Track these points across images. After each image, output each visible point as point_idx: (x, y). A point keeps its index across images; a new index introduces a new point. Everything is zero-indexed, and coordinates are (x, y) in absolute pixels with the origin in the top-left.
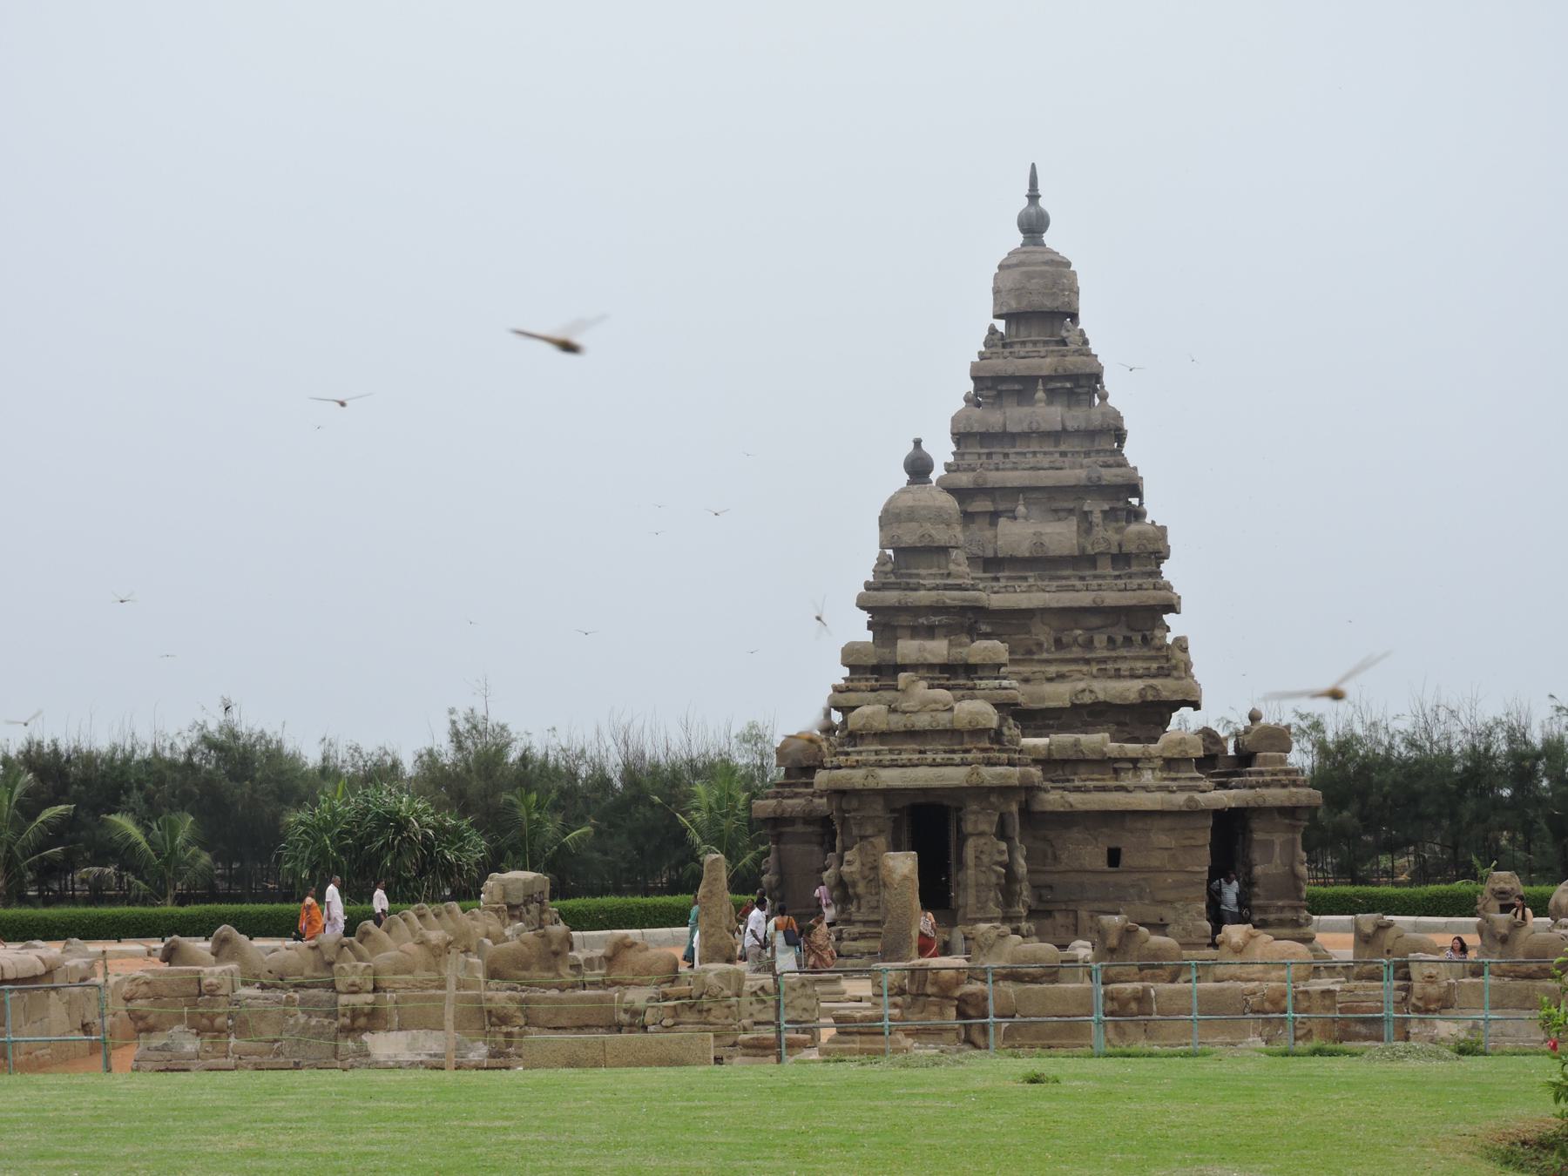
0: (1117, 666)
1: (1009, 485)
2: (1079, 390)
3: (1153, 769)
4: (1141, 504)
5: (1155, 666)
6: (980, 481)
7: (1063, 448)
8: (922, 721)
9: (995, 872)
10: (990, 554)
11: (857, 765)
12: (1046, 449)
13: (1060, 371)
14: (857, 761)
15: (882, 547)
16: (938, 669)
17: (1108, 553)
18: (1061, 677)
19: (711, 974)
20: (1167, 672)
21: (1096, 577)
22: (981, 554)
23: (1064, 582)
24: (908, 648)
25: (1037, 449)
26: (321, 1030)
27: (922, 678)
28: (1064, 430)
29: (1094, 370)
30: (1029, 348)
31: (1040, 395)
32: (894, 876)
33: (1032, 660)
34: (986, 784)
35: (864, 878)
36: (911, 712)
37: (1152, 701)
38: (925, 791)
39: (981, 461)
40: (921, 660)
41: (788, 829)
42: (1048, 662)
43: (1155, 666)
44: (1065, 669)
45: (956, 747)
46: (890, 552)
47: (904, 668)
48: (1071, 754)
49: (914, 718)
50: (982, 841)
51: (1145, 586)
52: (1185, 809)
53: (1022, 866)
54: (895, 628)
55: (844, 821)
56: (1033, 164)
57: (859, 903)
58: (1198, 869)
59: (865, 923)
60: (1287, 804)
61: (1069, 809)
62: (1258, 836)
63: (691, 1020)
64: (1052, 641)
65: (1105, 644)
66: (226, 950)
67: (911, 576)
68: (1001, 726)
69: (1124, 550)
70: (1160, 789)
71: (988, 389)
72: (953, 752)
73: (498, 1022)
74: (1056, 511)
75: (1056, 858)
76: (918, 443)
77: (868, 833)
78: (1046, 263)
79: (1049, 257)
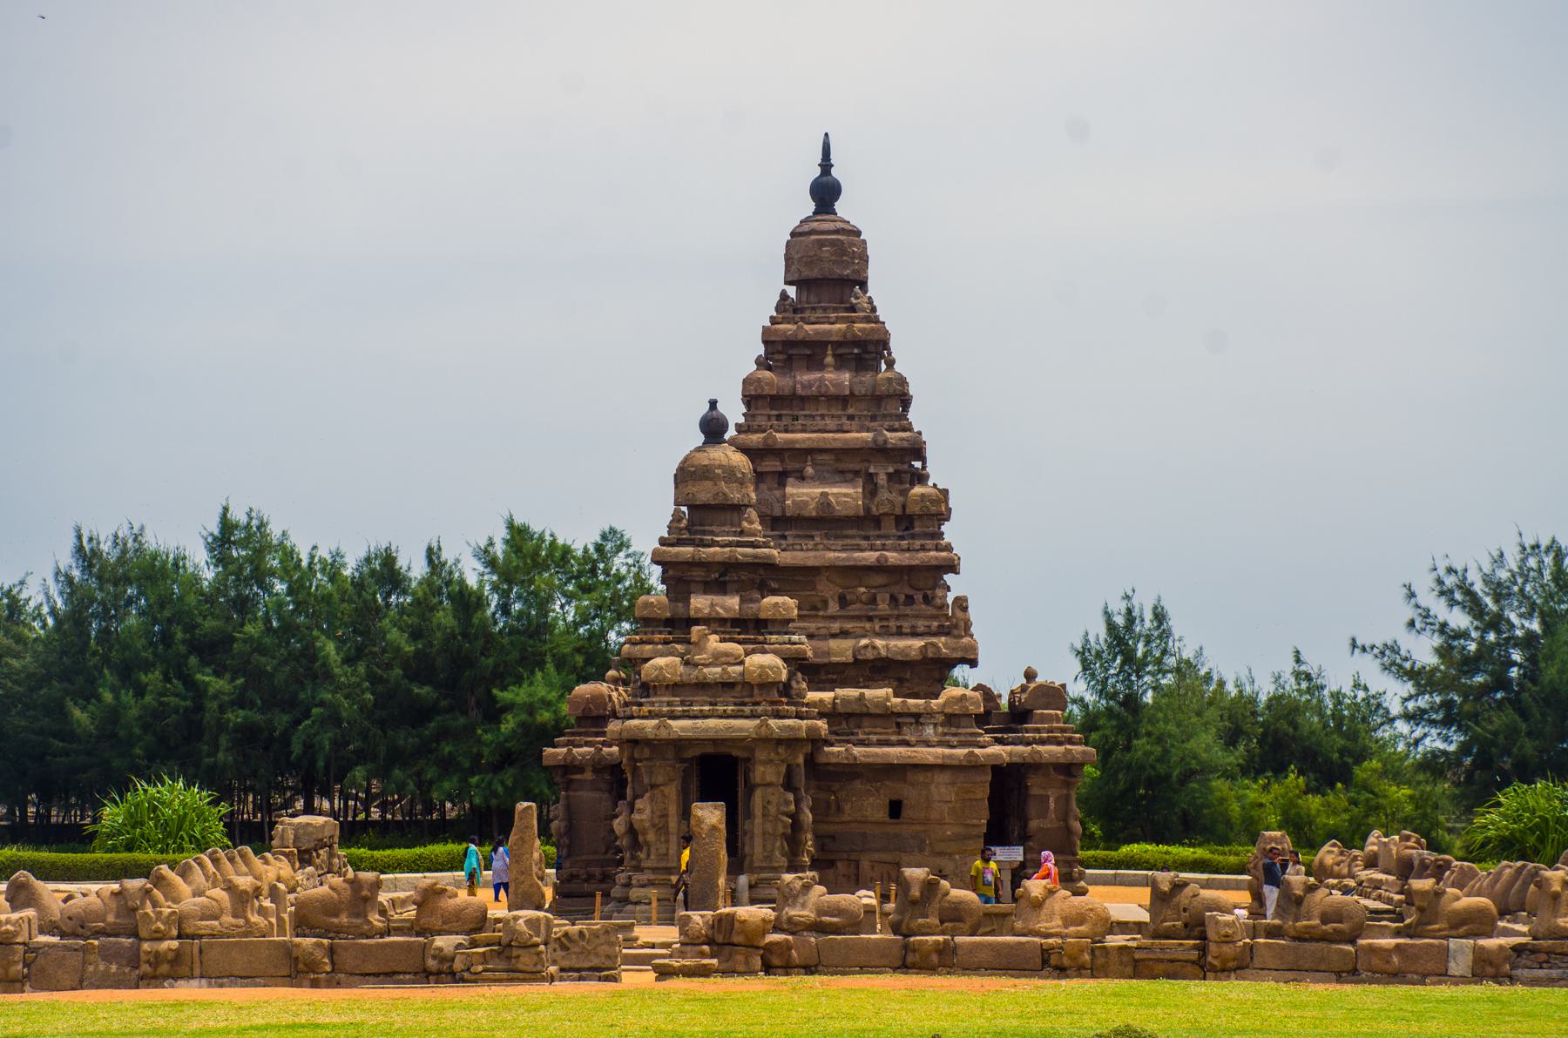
2: (867, 356)
4: (924, 467)
5: (936, 624)
6: (770, 442)
7: (851, 411)
8: (714, 672)
9: (782, 821)
10: (777, 512)
11: (650, 716)
13: (849, 337)
14: (650, 711)
15: (677, 503)
16: (729, 625)
17: (892, 514)
18: (844, 634)
19: (521, 921)
20: (946, 630)
21: (879, 537)
22: (769, 512)
23: (849, 541)
24: (700, 603)
25: (825, 412)
26: (121, 977)
27: (715, 632)
28: (852, 394)
29: (882, 337)
30: (819, 314)
31: (829, 360)
32: (703, 826)
33: (817, 616)
34: (774, 736)
35: (654, 826)
36: (704, 665)
37: (932, 658)
38: (715, 742)
39: (770, 423)
41: (578, 777)
42: (833, 618)
43: (936, 624)
44: (849, 626)
45: (746, 700)
46: (684, 509)
47: (697, 622)
48: (856, 708)
49: (705, 670)
50: (770, 790)
52: (964, 763)
53: (808, 817)
54: (688, 582)
55: (635, 770)
56: (826, 134)
57: (649, 850)
58: (975, 822)
59: (654, 870)
60: (1062, 760)
61: (852, 762)
62: (1035, 791)
63: (500, 967)
64: (836, 598)
66: (22, 896)
67: (704, 533)
68: (789, 679)
69: (908, 511)
70: (941, 744)
72: (744, 704)
73: (305, 969)
74: (842, 472)
75: (839, 810)
76: (713, 404)
77: (658, 783)
78: (837, 232)
79: (840, 225)
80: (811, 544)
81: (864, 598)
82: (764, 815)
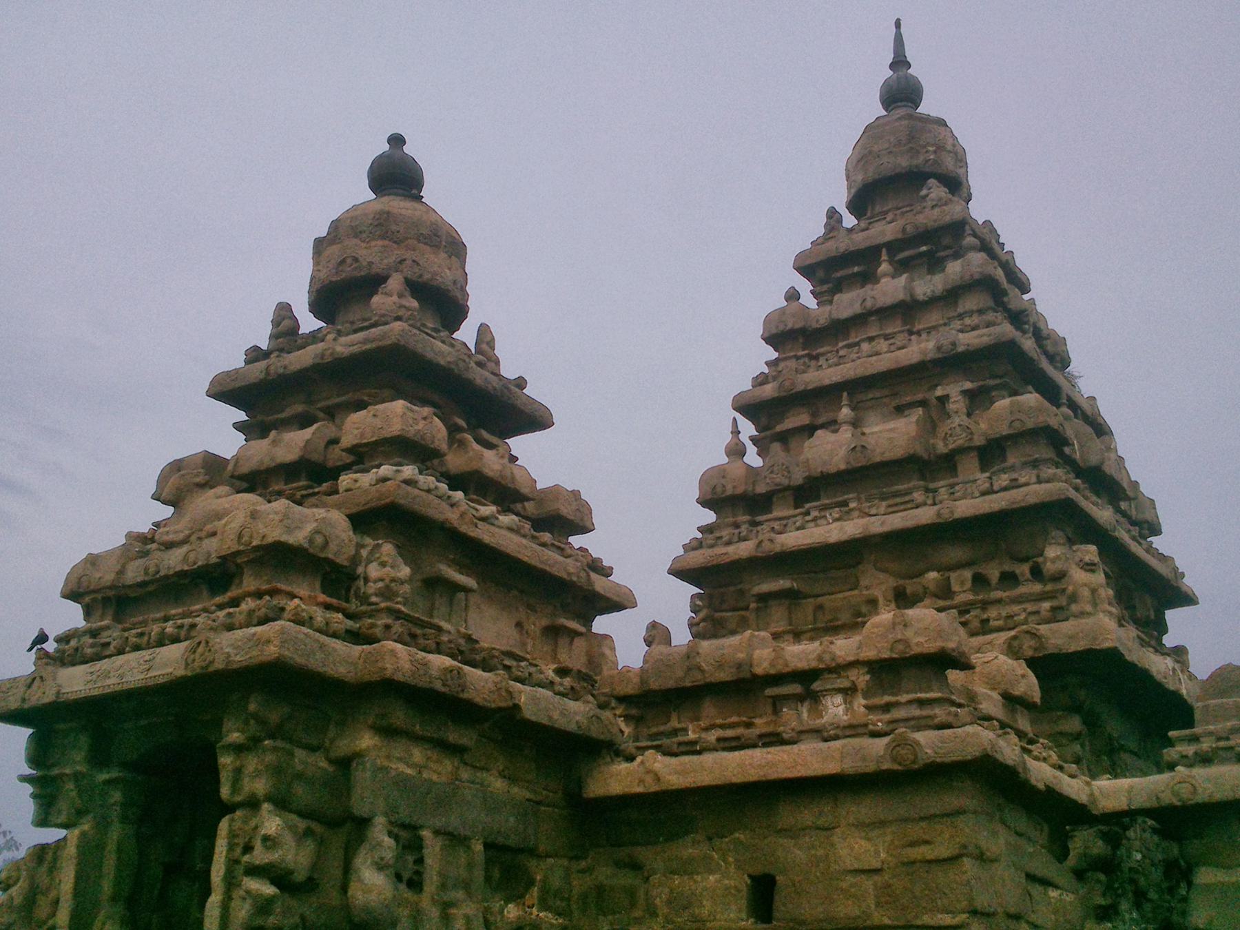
0: (985, 616)
1: (827, 382)
2: (942, 254)
3: (849, 692)
6: (787, 383)
7: (918, 327)
10: (798, 478)
12: (889, 331)
17: (970, 449)
22: (786, 482)
23: (898, 500)
25: (874, 334)
31: (884, 267)
34: (219, 665)
40: (268, 463)
43: (1046, 605)
51: (1022, 480)
61: (654, 788)
64: (890, 595)
65: (968, 584)
70: (854, 730)
71: (822, 282)
80: (836, 513)
81: (932, 587)
82: (231, 883)
